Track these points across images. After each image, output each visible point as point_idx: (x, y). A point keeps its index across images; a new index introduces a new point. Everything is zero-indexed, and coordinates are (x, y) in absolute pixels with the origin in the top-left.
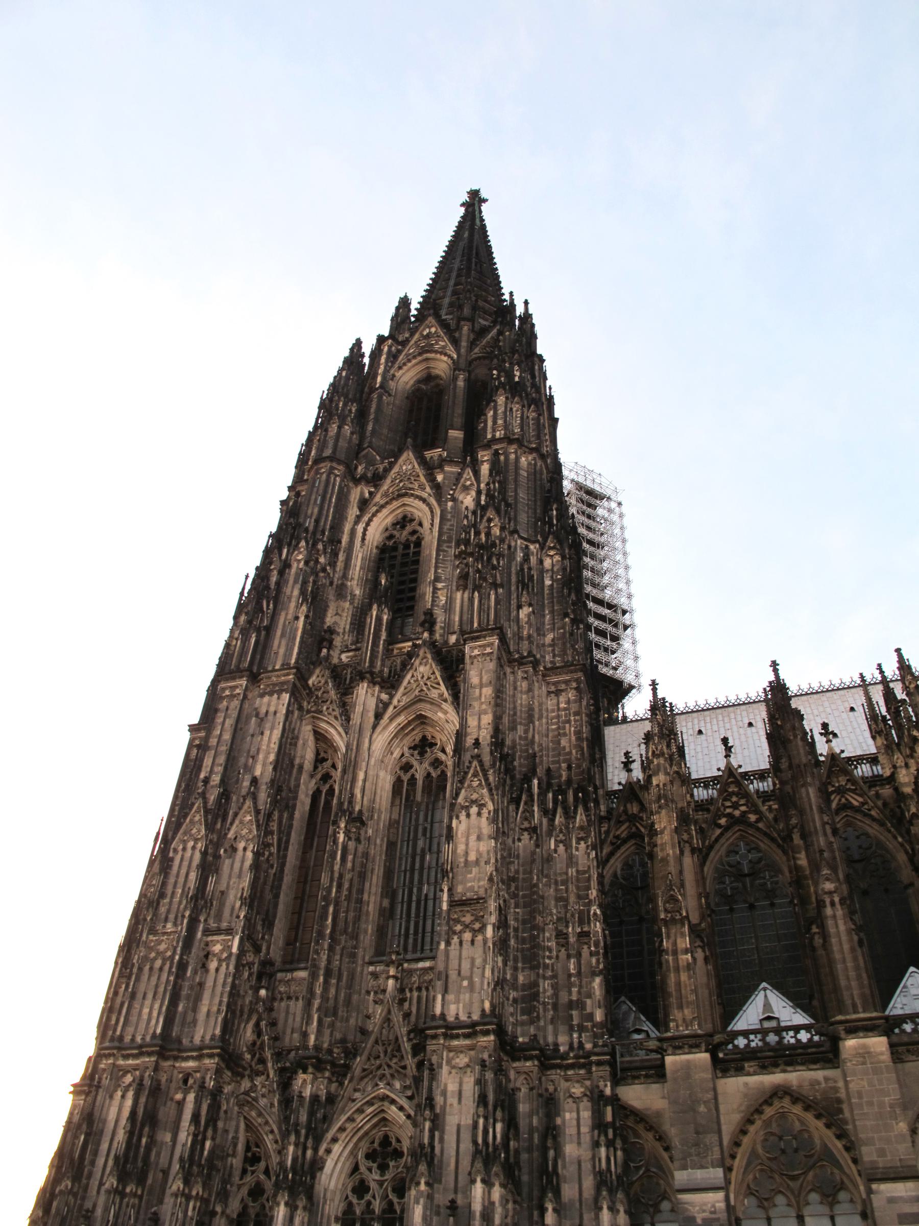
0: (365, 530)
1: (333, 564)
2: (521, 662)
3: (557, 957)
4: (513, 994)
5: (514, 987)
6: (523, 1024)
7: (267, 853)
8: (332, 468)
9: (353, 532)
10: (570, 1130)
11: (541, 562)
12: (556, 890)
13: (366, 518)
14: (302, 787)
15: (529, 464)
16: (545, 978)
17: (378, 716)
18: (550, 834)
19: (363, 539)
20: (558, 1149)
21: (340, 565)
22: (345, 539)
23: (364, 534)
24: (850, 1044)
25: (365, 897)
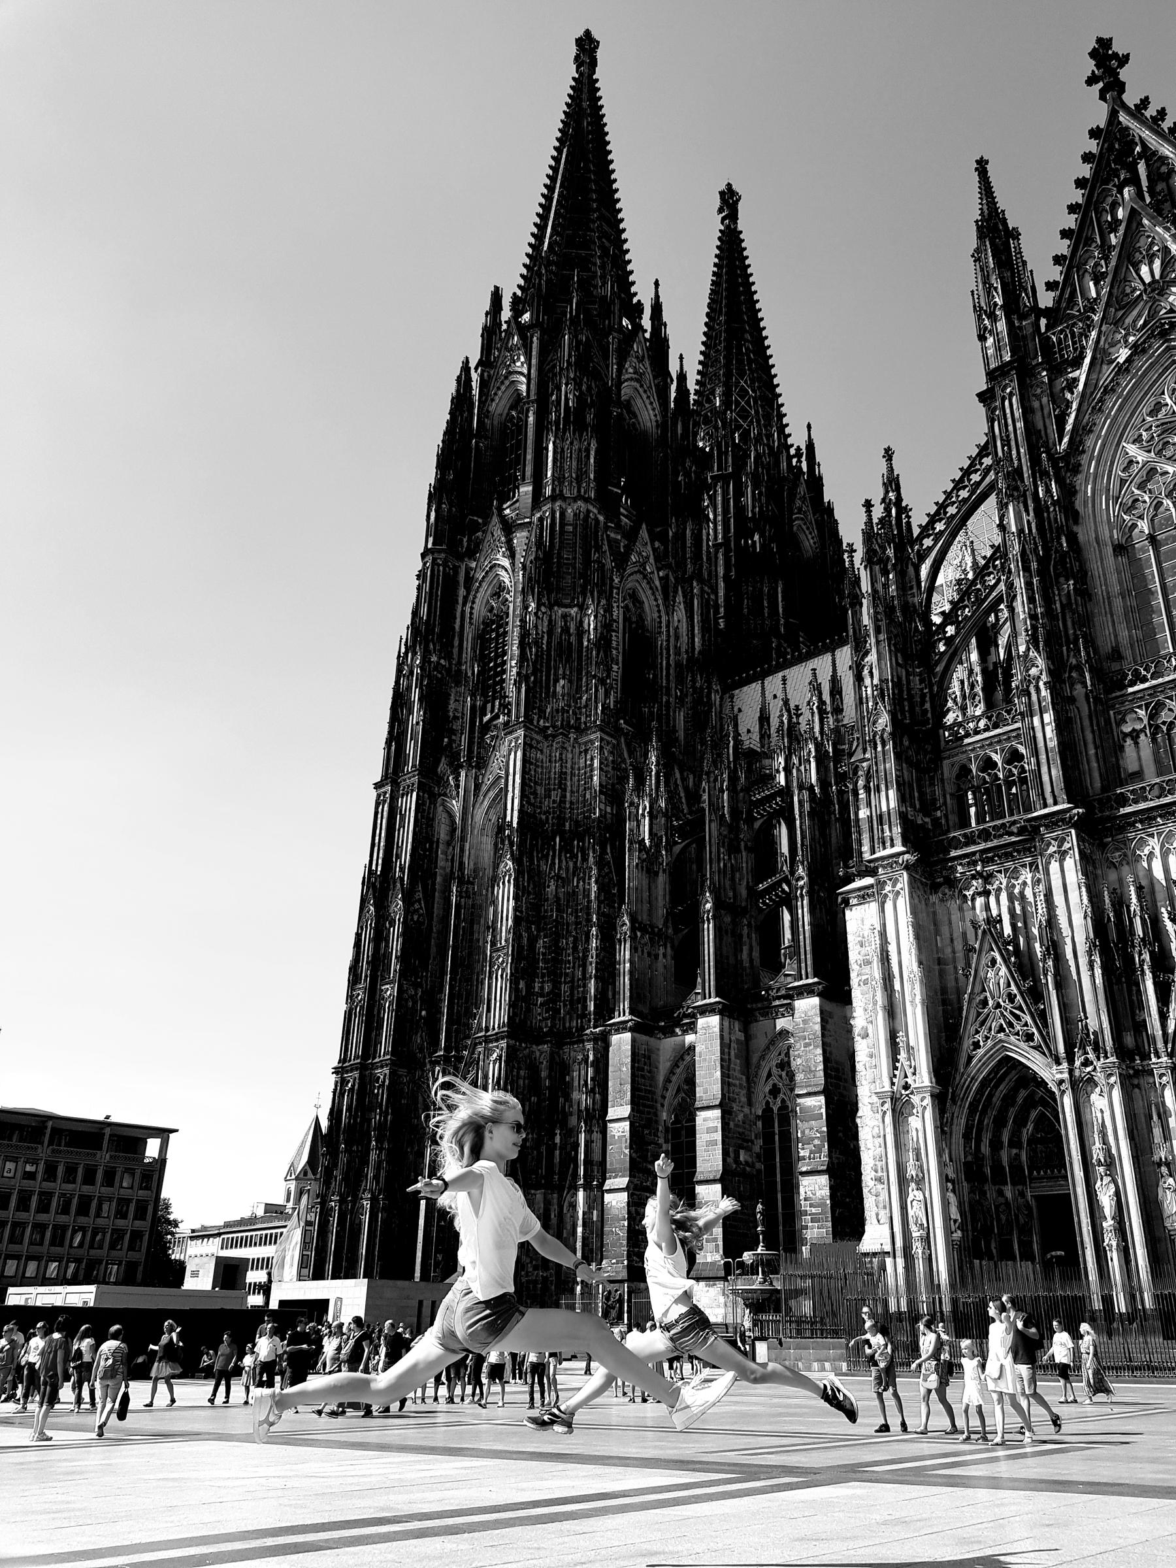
0: (472, 608)
1: (448, 656)
2: (554, 736)
3: (574, 967)
4: (540, 1000)
5: (542, 995)
6: (546, 1019)
7: (415, 917)
8: (434, 560)
9: (463, 612)
10: (576, 1084)
11: (581, 622)
12: (577, 917)
13: (471, 597)
14: (440, 855)
15: (575, 515)
16: (565, 983)
17: (476, 795)
18: (574, 875)
19: (471, 618)
20: (568, 1098)
21: (455, 651)
22: (457, 626)
23: (471, 613)
24: (701, 1022)
25: (476, 936)
